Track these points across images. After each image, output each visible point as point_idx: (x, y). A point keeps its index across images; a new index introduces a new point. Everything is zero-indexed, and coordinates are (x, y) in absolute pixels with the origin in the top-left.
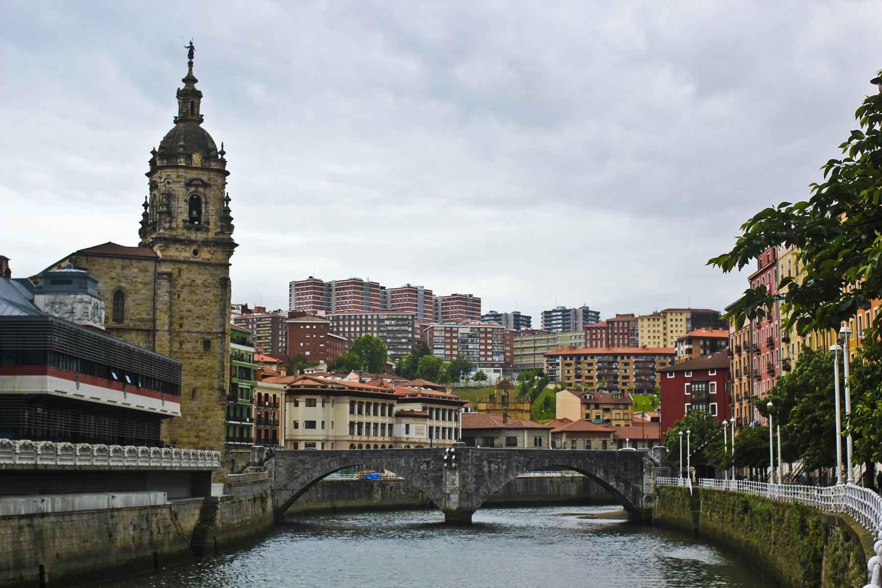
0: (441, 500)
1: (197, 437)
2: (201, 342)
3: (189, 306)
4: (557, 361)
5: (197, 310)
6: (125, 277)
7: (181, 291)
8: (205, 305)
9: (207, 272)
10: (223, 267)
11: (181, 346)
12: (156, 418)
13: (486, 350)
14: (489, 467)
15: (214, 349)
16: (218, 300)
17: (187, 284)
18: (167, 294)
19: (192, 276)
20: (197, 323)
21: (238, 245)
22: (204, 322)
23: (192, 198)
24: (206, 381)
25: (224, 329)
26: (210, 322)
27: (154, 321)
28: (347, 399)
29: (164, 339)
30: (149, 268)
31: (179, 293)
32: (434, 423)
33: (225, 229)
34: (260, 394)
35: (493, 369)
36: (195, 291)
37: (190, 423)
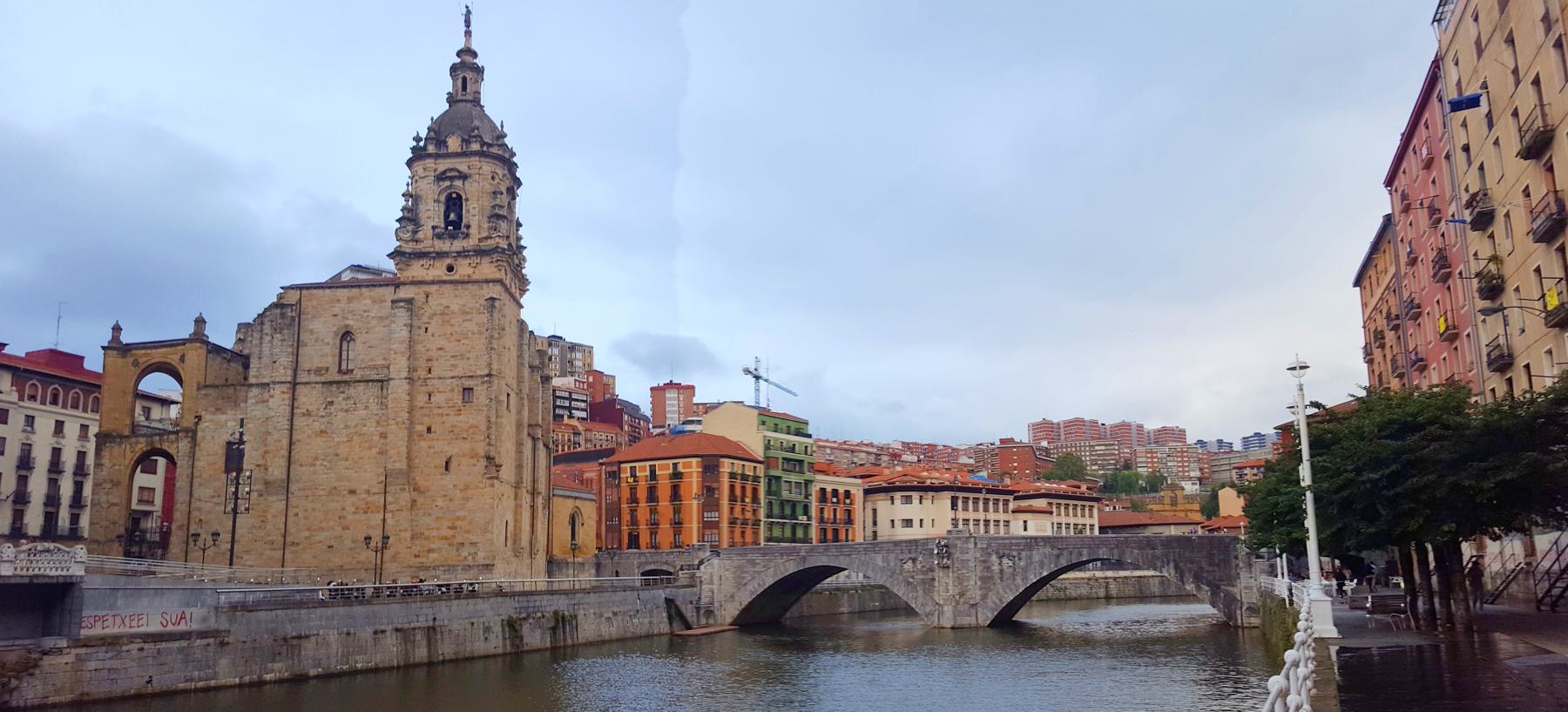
1: (453, 528)
2: (458, 392)
6: (352, 312)
7: (429, 323)
8: (464, 338)
9: (467, 293)
10: (491, 284)
11: (430, 399)
15: (478, 399)
17: (439, 312)
18: (405, 328)
19: (444, 302)
20: (452, 365)
23: (449, 198)
24: (466, 446)
26: (471, 362)
29: (400, 391)
30: (386, 297)
31: (427, 325)
37: (442, 508)
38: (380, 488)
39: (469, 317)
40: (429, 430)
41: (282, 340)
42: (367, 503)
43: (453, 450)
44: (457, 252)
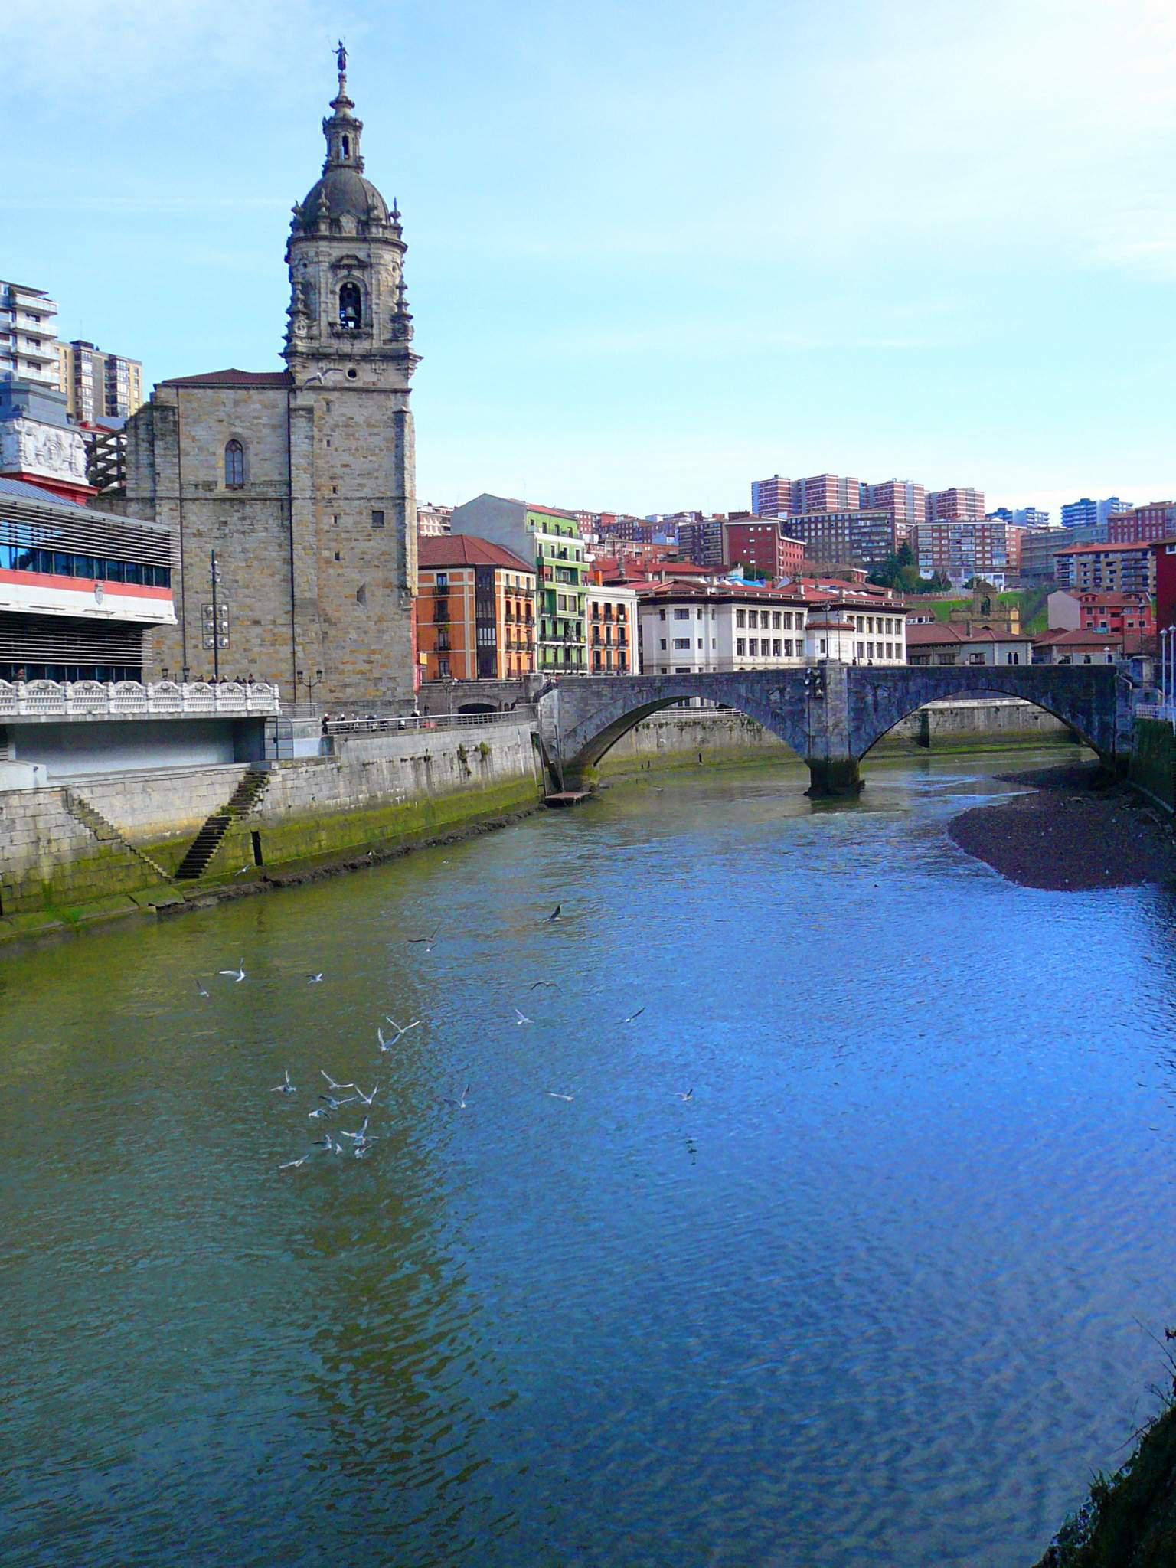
4: (1071, 561)
5: (359, 464)
9: (371, 403)
12: (131, 631)
13: (984, 552)
14: (875, 695)
19: (348, 412)
20: (360, 485)
21: (421, 358)
23: (344, 288)
25: (403, 493)
26: (380, 481)
27: (289, 484)
28: (735, 608)
29: (305, 512)
32: (865, 637)
34: (595, 605)
36: (353, 435)
37: (355, 641)
38: (284, 619)
39: (375, 430)
40: (337, 558)
41: (165, 449)
42: (274, 635)
43: (369, 577)
44: (361, 356)
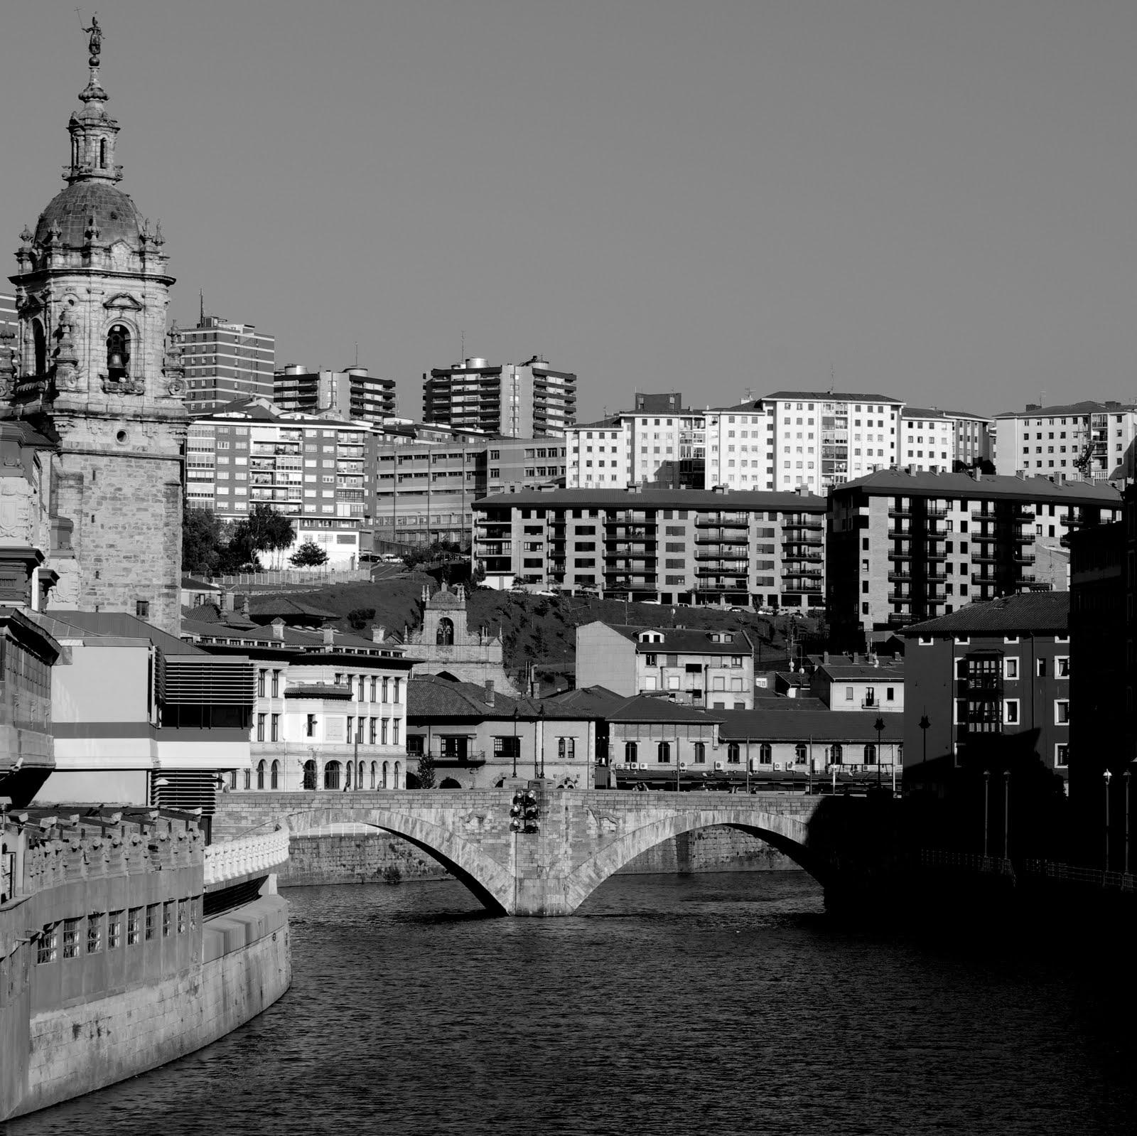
0: (505, 891)
3: (111, 537)
5: (125, 545)
8: (139, 534)
9: (142, 471)
14: (600, 827)
16: (161, 525)
19: (114, 480)
20: (125, 569)
22: (137, 567)
23: (111, 332)
26: (147, 566)
33: (173, 391)
35: (335, 534)
36: (121, 509)
